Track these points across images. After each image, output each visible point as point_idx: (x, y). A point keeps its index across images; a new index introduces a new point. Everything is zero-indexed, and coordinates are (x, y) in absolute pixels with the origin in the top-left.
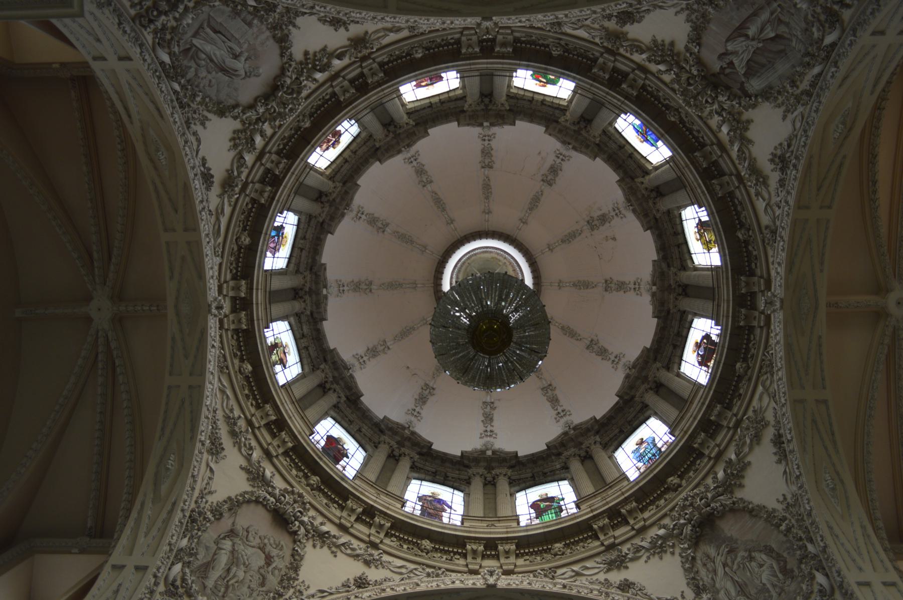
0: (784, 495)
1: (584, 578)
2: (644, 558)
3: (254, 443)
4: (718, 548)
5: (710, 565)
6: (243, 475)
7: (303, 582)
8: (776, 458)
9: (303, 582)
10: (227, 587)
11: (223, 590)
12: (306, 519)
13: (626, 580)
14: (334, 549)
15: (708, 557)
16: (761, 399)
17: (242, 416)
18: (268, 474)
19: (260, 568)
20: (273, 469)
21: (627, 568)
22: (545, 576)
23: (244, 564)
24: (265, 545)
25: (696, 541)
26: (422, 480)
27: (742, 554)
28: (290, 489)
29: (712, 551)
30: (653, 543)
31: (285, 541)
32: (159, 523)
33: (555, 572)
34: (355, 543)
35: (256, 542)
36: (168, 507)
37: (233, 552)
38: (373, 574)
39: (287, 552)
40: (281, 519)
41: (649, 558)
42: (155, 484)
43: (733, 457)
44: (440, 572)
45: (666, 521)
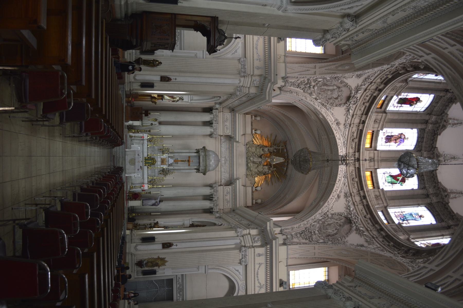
0: (348, 242)
1: (343, 186)
2: (346, 203)
3: (367, 85)
4: (342, 223)
5: (339, 219)
6: (356, 85)
7: (334, 109)
8: (359, 244)
9: (334, 109)
10: (324, 91)
11: (323, 90)
12: (351, 105)
13: (340, 197)
14: (346, 115)
15: (341, 219)
16: (376, 245)
17: (372, 80)
18: (360, 92)
19: (333, 97)
20: (362, 93)
21: (344, 198)
22: (345, 175)
23: (332, 93)
24: (340, 96)
25: (346, 218)
26: (418, 133)
27: (338, 228)
28: (358, 99)
29: (342, 221)
30: (349, 206)
31: (344, 101)
32: (329, 71)
33: (346, 178)
34: (349, 120)
35: (340, 94)
36: (334, 72)
37: (334, 89)
38: (342, 127)
39: (341, 103)
40: (348, 98)
41: (346, 204)
42: (341, 65)
43: (365, 233)
44: (345, 145)
45: (355, 211)
